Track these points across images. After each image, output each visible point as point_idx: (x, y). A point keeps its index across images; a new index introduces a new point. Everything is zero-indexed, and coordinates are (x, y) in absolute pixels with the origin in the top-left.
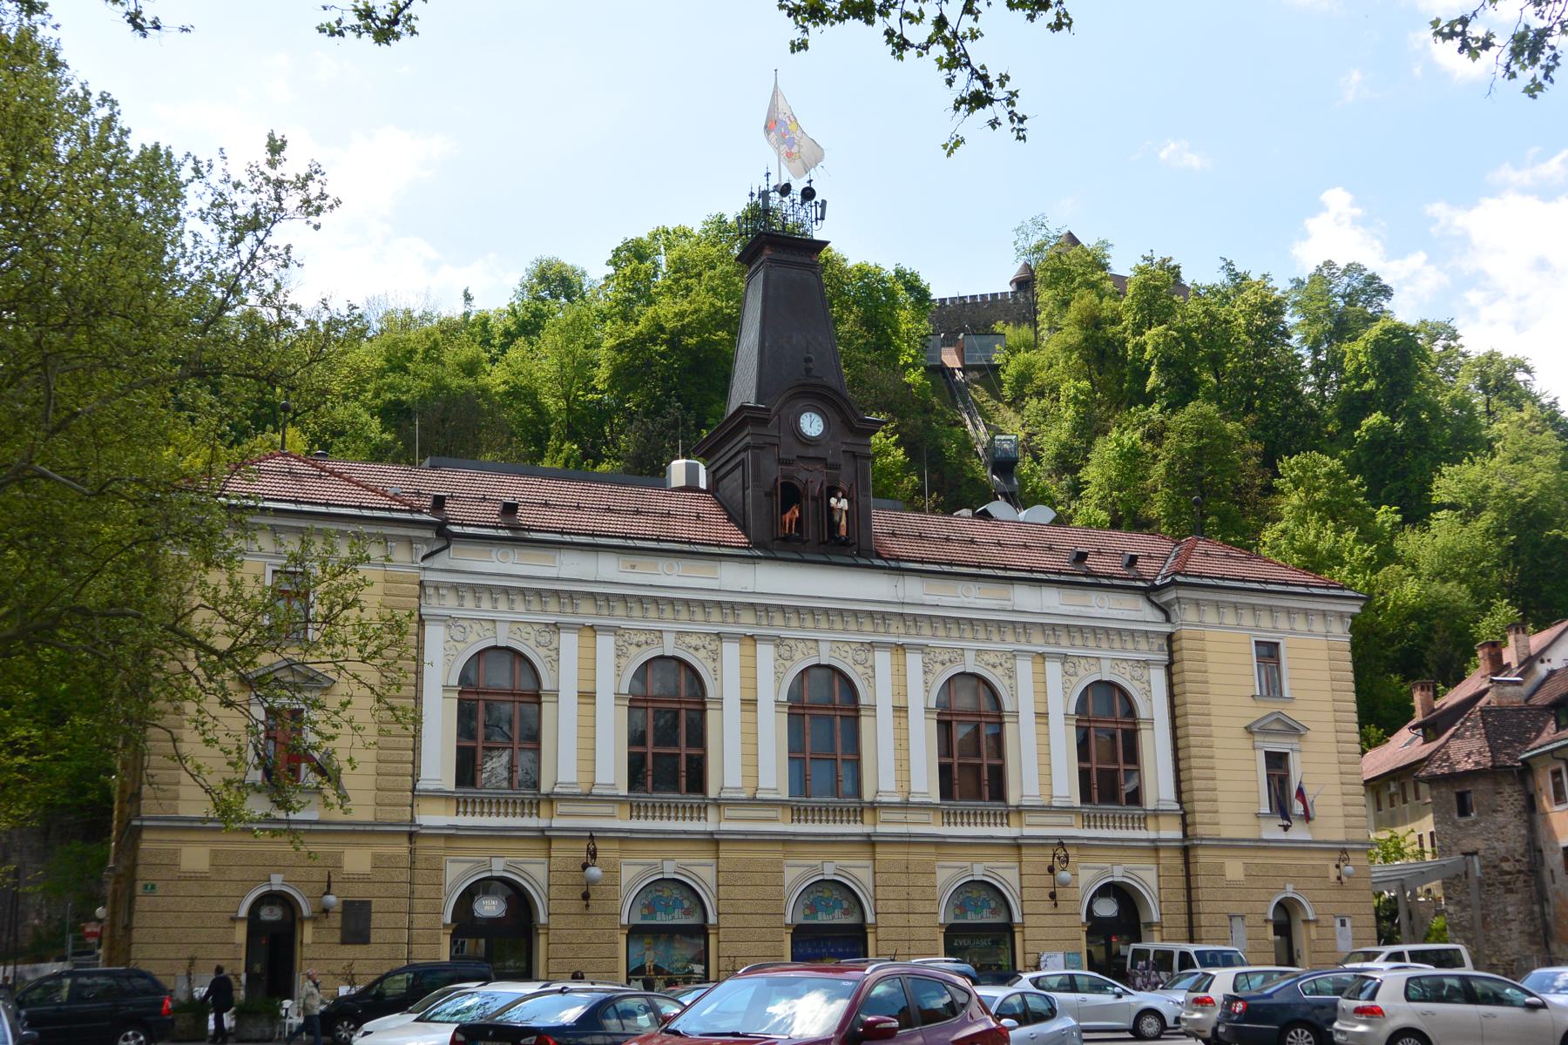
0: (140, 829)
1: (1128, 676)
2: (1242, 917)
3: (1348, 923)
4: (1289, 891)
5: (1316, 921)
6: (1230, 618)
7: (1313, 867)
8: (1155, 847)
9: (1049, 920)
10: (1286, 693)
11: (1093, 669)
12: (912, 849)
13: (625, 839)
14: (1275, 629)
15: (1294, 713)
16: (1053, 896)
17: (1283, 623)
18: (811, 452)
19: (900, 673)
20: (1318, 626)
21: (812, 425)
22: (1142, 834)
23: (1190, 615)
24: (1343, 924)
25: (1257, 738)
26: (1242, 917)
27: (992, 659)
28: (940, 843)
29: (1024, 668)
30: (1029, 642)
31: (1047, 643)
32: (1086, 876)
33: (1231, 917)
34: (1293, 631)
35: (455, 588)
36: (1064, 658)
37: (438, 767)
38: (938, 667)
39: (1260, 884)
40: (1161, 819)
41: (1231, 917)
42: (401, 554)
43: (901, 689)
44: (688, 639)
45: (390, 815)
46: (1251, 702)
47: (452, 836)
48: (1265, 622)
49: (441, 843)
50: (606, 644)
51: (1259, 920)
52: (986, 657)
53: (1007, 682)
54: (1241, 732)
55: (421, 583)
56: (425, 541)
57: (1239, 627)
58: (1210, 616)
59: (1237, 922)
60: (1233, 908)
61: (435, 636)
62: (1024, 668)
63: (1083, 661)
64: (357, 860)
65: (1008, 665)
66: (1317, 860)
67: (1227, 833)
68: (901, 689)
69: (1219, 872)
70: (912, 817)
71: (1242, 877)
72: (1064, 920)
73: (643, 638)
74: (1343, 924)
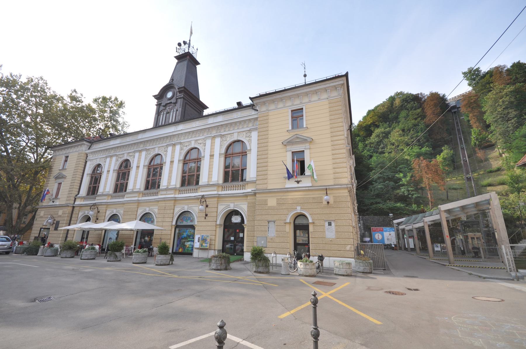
0: (38, 208)
1: (244, 137)
2: (274, 222)
3: (333, 224)
4: (299, 210)
5: (313, 223)
6: (281, 105)
7: (314, 198)
8: (246, 195)
9: (204, 224)
10: (305, 126)
14: (301, 103)
15: (306, 134)
16: (206, 215)
17: (306, 100)
18: (169, 102)
19: (173, 152)
20: (325, 96)
21: (170, 95)
22: (244, 191)
23: (264, 109)
24: (330, 224)
25: (288, 147)
26: (274, 222)
27: (200, 142)
29: (208, 142)
30: (211, 134)
31: (217, 133)
32: (223, 208)
33: (269, 222)
34: (310, 101)
35: (92, 153)
37: (84, 191)
38: (185, 148)
39: (284, 207)
40: (249, 185)
41: (269, 222)
42: (81, 149)
43: (173, 157)
44: (130, 154)
45: (68, 202)
46: (287, 134)
47: (81, 206)
48: (297, 102)
49: (78, 208)
50: (114, 159)
53: (204, 147)
54: (281, 146)
57: (285, 107)
58: (272, 107)
59: (271, 225)
60: (270, 218)
61: (88, 164)
62: (208, 142)
63: (229, 136)
64: (60, 212)
66: (316, 194)
67: (270, 187)
68: (173, 157)
69: (265, 203)
70: (169, 192)
71: (275, 205)
72: (209, 224)
73: (122, 156)
74: (330, 224)
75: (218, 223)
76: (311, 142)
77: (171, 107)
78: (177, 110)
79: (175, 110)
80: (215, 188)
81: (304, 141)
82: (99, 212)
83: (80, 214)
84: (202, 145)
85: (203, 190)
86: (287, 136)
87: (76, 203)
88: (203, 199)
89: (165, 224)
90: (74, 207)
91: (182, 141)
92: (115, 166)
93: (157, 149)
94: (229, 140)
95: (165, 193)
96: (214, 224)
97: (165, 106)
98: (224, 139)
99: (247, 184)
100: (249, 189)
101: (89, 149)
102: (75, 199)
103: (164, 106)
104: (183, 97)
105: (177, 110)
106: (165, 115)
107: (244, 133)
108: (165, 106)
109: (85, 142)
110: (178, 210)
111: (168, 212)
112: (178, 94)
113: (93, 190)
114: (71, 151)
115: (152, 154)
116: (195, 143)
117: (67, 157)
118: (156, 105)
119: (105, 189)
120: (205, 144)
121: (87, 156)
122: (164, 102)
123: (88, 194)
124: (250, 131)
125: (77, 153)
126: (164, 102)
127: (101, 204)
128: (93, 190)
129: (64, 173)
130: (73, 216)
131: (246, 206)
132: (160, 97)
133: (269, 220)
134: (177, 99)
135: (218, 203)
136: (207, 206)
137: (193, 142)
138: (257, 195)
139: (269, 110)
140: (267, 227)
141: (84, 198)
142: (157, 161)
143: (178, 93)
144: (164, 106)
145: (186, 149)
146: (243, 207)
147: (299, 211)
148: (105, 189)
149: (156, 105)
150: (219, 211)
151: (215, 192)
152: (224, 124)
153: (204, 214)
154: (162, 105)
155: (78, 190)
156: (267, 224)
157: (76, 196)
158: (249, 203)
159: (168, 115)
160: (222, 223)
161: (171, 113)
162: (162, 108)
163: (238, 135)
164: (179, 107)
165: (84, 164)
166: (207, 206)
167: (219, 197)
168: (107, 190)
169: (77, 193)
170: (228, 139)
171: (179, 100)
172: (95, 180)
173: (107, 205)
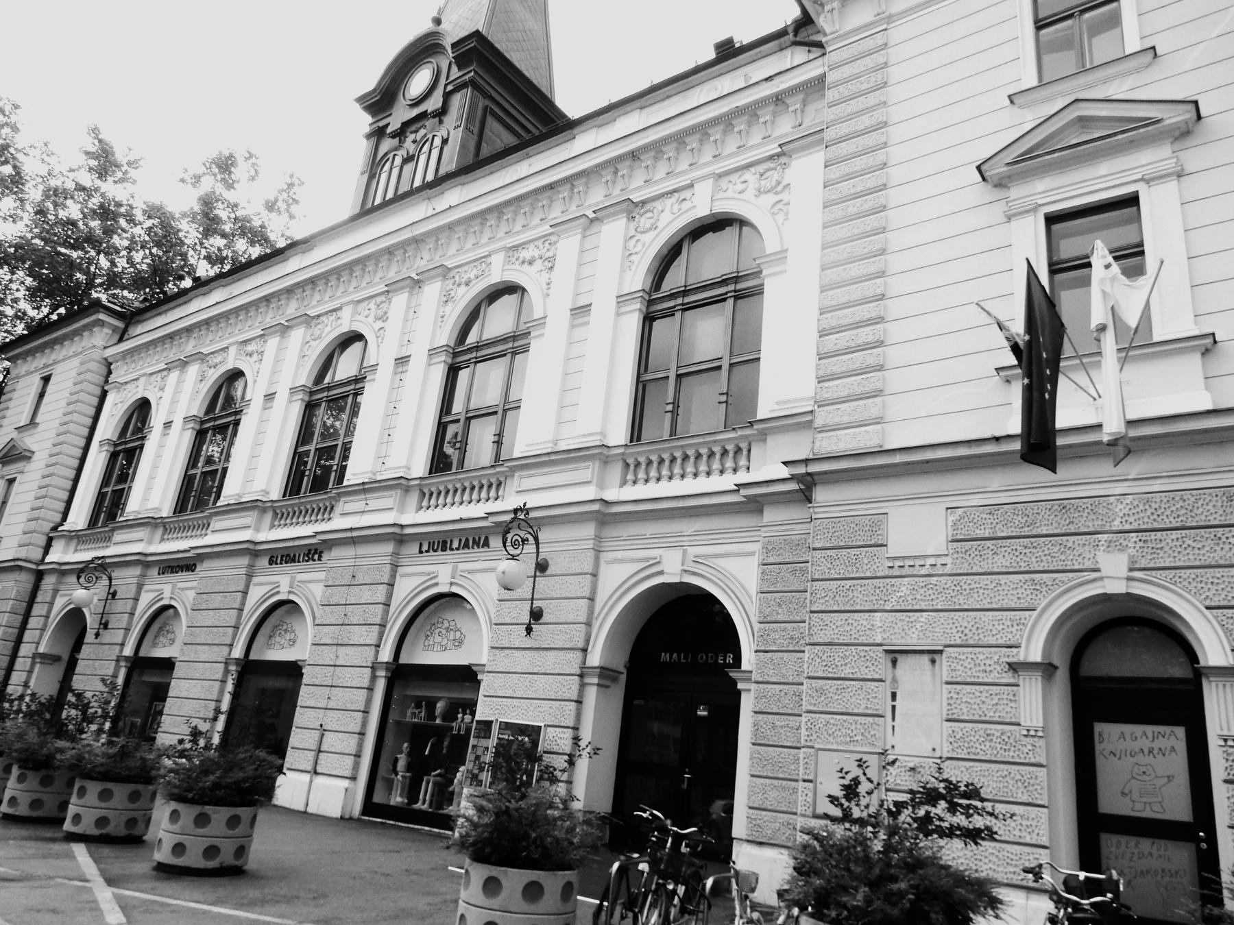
1: (751, 191)
2: (933, 654)
8: (753, 503)
9: (523, 661)
11: (686, 206)
12: (363, 550)
13: (143, 562)
16: (536, 615)
19: (412, 311)
21: (419, 81)
28: (399, 537)
32: (626, 574)
33: (895, 655)
36: (632, 208)
38: (463, 289)
39: (1000, 563)
41: (895, 655)
45: (22, 553)
47: (62, 571)
51: (992, 665)
52: (525, 254)
53: (545, 276)
54: (982, 192)
55: (106, 359)
56: (102, 323)
59: (912, 672)
61: (110, 399)
63: (669, 202)
65: (550, 254)
70: (374, 504)
72: (549, 661)
73: (218, 359)
75: (595, 658)
76: (1183, 134)
77: (422, 132)
78: (445, 141)
79: (437, 141)
80: (587, 471)
81: (1132, 131)
82: (114, 594)
83: (60, 602)
84: (539, 264)
85: (528, 483)
86: (1004, 127)
87: (48, 559)
88: (520, 527)
89: (346, 655)
90: (40, 575)
91: (450, 263)
92: (192, 400)
93: (346, 313)
94: (670, 221)
95: (359, 506)
96: (572, 662)
97: (400, 134)
98: (644, 222)
99: (763, 436)
100: (768, 465)
101: (121, 340)
102: (50, 541)
103: (394, 135)
104: (472, 83)
105: (445, 141)
106: (395, 172)
107: (749, 175)
108: (400, 134)
109: (102, 316)
110: (412, 584)
111: (366, 595)
112: (455, 73)
113: (109, 506)
114: (60, 352)
115: (331, 331)
116: (508, 260)
117: (46, 380)
118: (369, 136)
119: (145, 499)
120: (552, 259)
121: (110, 372)
122: (400, 114)
123: (93, 523)
124: (782, 155)
125: (75, 362)
126: (400, 114)
127: (124, 562)
128: (109, 506)
129: (30, 441)
130: (38, 610)
131: (755, 561)
132: (380, 101)
133: (898, 641)
134: (447, 96)
135: (598, 552)
136: (542, 567)
137: (498, 260)
138: (821, 495)
139: (890, 19)
140: (884, 690)
141: (77, 538)
142: (345, 367)
143: (454, 68)
144: (394, 135)
145: (465, 297)
146: (734, 574)
147: (1116, 587)
148: (145, 499)
149: (369, 136)
150: (601, 598)
151: (589, 493)
152: (645, 148)
153: (527, 606)
154: (389, 130)
155: (61, 506)
156: (882, 667)
157: (55, 529)
158: (767, 550)
159: (408, 168)
160: (620, 662)
161: (423, 158)
162: (387, 144)
163: (717, 189)
164: (453, 129)
165: (95, 401)
166: (542, 567)
167: (605, 517)
168: (153, 503)
169: (58, 518)
170: (665, 218)
171: (457, 100)
172: (125, 457)
173: (147, 565)
